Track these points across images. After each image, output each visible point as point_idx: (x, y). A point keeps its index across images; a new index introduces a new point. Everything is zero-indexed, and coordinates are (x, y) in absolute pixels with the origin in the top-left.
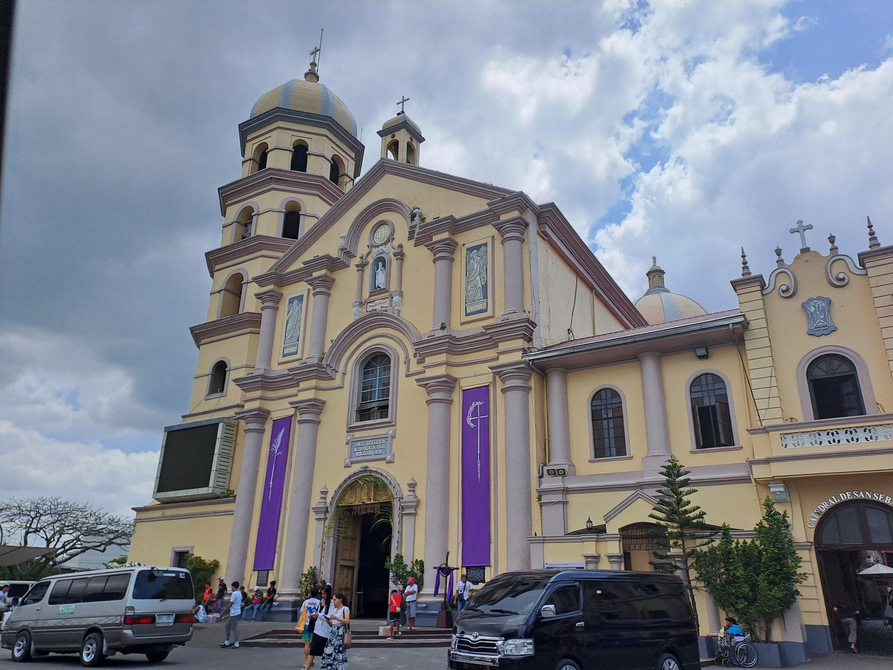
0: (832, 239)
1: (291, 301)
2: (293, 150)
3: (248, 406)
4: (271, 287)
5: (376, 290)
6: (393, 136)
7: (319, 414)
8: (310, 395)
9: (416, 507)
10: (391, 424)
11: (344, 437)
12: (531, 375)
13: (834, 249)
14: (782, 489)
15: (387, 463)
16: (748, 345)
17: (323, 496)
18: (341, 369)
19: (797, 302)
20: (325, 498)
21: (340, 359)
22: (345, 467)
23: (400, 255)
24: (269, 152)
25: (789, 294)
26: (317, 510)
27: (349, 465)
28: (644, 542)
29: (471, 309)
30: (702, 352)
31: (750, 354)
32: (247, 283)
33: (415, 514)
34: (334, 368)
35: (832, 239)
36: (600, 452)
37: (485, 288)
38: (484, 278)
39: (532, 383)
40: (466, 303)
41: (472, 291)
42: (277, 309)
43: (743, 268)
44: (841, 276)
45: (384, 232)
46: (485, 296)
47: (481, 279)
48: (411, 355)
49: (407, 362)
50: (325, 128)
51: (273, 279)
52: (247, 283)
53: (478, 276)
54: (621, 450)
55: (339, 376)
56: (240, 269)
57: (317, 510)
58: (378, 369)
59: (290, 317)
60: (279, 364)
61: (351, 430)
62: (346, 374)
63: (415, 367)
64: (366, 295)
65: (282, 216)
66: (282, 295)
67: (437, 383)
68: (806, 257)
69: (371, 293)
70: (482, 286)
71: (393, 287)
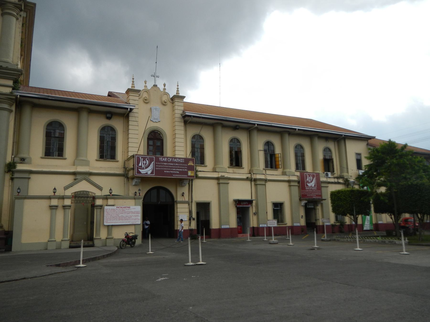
0: (165, 85)
12: (14, 103)
13: (165, 89)
14: (140, 181)
16: (130, 119)
19: (148, 106)
25: (146, 101)
28: (74, 200)
30: (109, 115)
31: (130, 123)
35: (165, 85)
36: (48, 153)
39: (13, 108)
43: (132, 84)
44: (166, 101)
54: (60, 153)
68: (155, 88)
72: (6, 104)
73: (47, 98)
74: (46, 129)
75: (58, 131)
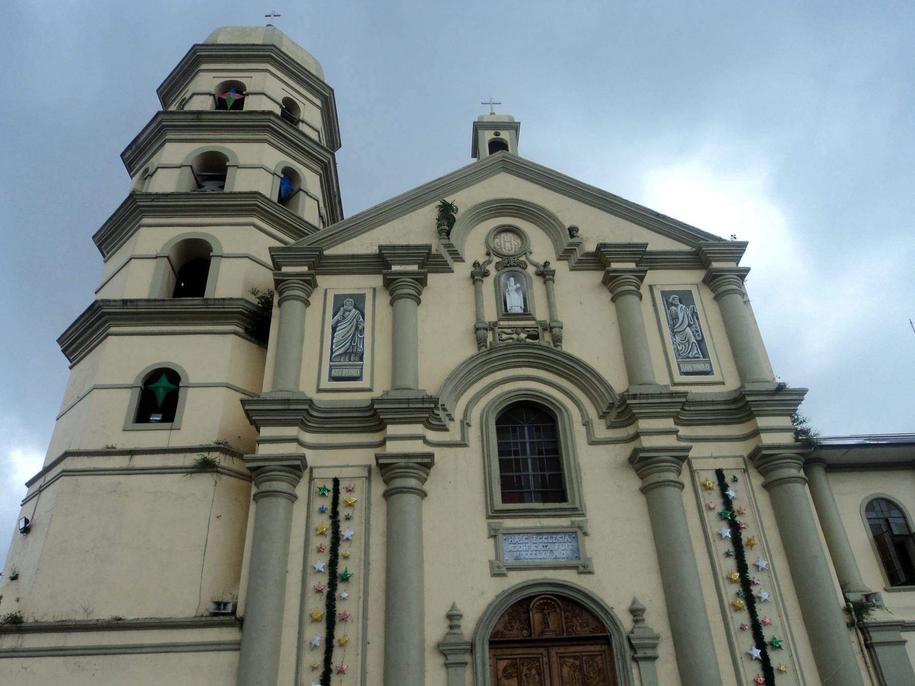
1: (339, 300)
2: (284, 107)
3: (264, 450)
4: (304, 269)
5: (507, 315)
6: (497, 134)
7: (423, 481)
8: (417, 447)
9: (654, 647)
10: (577, 511)
11: (482, 524)
15: (580, 573)
17: (455, 622)
18: (458, 414)
20: (459, 627)
21: (457, 400)
22: (494, 575)
23: (545, 274)
24: (248, 94)
26: (443, 649)
27: (504, 570)
29: (688, 368)
32: (222, 257)
33: (654, 658)
34: (448, 413)
37: (701, 342)
38: (697, 332)
40: (677, 358)
41: (683, 344)
42: (307, 304)
45: (508, 243)
46: (705, 355)
47: (693, 332)
48: (592, 412)
49: (587, 424)
50: (321, 100)
51: (312, 258)
52: (222, 257)
53: (688, 329)
55: (455, 428)
56: (203, 233)
57: (443, 649)
58: (526, 429)
59: (338, 322)
60: (320, 391)
61: (494, 514)
62: (470, 426)
63: (601, 430)
64: (490, 314)
65: (278, 181)
66: (316, 286)
67: (672, 458)
69: (504, 315)
70: (696, 340)
71: (541, 314)
72: (790, 467)
73: (868, 442)
74: (867, 519)
75: (891, 520)
